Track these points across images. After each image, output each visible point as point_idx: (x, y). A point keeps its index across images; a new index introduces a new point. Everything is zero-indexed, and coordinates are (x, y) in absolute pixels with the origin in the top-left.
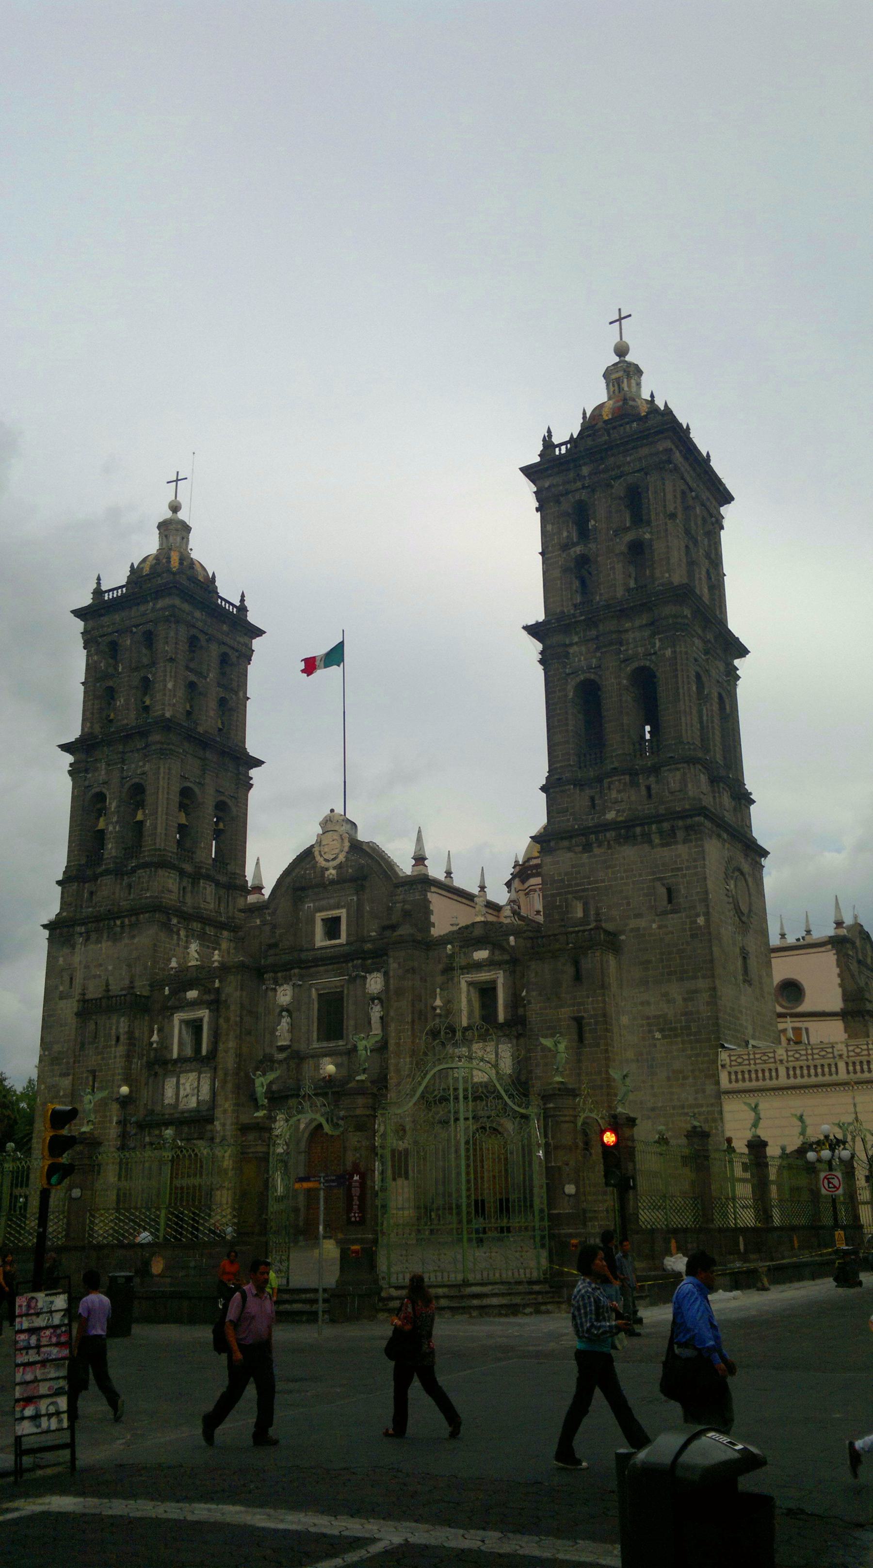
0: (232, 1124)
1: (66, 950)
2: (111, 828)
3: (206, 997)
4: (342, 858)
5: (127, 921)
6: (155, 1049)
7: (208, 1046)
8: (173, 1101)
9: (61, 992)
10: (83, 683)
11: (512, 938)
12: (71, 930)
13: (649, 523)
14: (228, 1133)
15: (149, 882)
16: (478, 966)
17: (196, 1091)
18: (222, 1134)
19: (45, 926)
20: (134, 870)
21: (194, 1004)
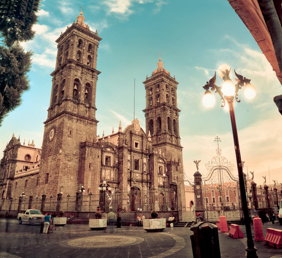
1: (70, 122)
2: (82, 92)
3: (112, 151)
4: (139, 130)
5: (89, 121)
9: (68, 134)
11: (165, 159)
12: (72, 116)
13: (175, 96)
14: (126, 187)
16: (160, 162)
20: (89, 108)
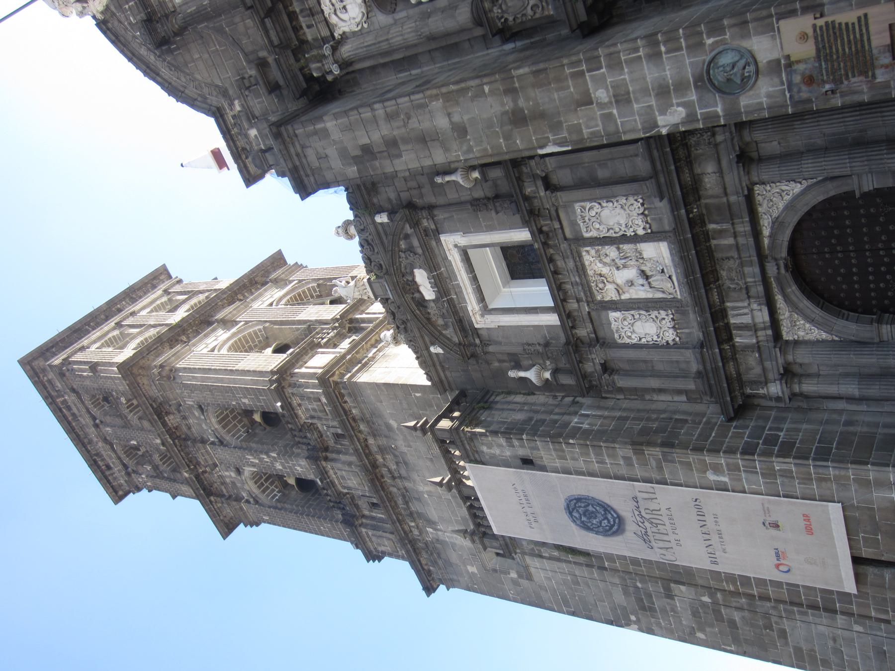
0: (655, 56)
2: (279, 466)
3: (416, 243)
5: (371, 441)
6: (555, 372)
7: (512, 227)
8: (666, 318)
9: (520, 576)
10: (174, 497)
15: (309, 398)
17: (626, 247)
18: (693, 96)
19: (429, 589)
21: (442, 283)
